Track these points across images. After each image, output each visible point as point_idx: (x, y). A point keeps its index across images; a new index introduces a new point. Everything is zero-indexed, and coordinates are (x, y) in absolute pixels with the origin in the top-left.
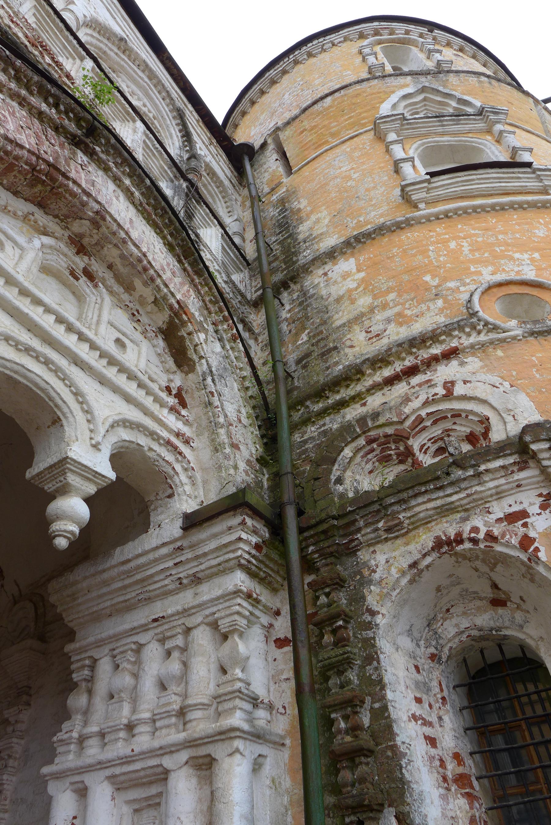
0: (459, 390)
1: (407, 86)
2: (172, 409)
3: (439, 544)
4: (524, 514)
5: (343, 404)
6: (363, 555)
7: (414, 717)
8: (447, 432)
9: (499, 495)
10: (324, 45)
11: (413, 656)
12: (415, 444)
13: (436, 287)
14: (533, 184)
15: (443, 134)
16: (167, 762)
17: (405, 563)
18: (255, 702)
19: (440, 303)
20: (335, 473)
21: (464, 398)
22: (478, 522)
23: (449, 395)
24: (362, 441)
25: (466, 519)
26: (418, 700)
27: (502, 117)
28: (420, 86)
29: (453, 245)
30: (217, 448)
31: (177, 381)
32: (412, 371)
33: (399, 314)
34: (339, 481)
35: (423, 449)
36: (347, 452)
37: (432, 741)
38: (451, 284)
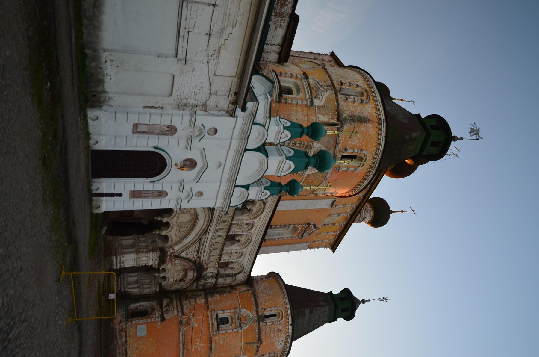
0: (172, 312)
1: (253, 315)
2: (174, 280)
3: (155, 308)
4: (156, 315)
5: (176, 300)
6: (156, 301)
7: (141, 305)
8: (168, 311)
9: (158, 313)
10: (285, 299)
11: (147, 305)
12: (168, 307)
13: (192, 313)
14: (214, 330)
15: (235, 320)
16: (139, 284)
17: (154, 305)
18: (143, 291)
19: (188, 312)
20: (166, 299)
21: (171, 312)
22: (156, 311)
23: (172, 311)
24: (170, 302)
25: (157, 310)
26: (142, 305)
27: (238, 331)
28: (253, 317)
29: (201, 316)
30: (170, 285)
31: (178, 280)
32: (177, 307)
33: (188, 307)
34: (165, 299)
35: (167, 308)
36: (169, 300)
37: (139, 306)
38: (191, 314)
